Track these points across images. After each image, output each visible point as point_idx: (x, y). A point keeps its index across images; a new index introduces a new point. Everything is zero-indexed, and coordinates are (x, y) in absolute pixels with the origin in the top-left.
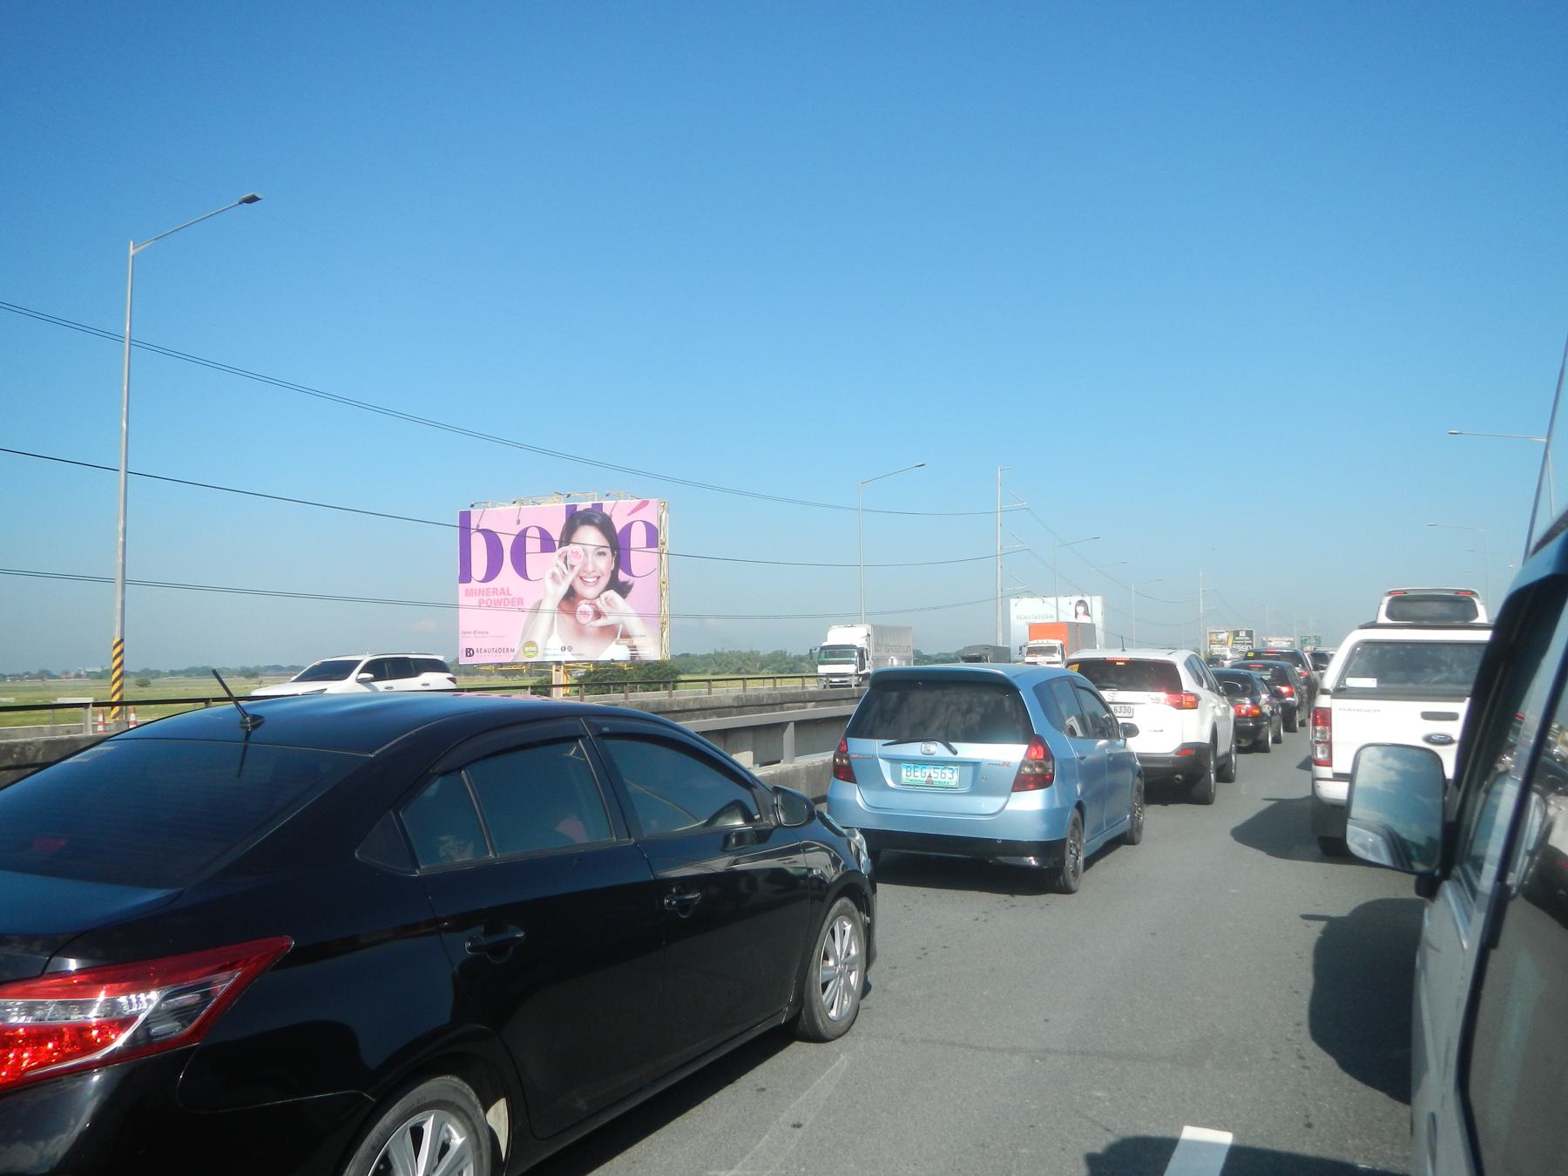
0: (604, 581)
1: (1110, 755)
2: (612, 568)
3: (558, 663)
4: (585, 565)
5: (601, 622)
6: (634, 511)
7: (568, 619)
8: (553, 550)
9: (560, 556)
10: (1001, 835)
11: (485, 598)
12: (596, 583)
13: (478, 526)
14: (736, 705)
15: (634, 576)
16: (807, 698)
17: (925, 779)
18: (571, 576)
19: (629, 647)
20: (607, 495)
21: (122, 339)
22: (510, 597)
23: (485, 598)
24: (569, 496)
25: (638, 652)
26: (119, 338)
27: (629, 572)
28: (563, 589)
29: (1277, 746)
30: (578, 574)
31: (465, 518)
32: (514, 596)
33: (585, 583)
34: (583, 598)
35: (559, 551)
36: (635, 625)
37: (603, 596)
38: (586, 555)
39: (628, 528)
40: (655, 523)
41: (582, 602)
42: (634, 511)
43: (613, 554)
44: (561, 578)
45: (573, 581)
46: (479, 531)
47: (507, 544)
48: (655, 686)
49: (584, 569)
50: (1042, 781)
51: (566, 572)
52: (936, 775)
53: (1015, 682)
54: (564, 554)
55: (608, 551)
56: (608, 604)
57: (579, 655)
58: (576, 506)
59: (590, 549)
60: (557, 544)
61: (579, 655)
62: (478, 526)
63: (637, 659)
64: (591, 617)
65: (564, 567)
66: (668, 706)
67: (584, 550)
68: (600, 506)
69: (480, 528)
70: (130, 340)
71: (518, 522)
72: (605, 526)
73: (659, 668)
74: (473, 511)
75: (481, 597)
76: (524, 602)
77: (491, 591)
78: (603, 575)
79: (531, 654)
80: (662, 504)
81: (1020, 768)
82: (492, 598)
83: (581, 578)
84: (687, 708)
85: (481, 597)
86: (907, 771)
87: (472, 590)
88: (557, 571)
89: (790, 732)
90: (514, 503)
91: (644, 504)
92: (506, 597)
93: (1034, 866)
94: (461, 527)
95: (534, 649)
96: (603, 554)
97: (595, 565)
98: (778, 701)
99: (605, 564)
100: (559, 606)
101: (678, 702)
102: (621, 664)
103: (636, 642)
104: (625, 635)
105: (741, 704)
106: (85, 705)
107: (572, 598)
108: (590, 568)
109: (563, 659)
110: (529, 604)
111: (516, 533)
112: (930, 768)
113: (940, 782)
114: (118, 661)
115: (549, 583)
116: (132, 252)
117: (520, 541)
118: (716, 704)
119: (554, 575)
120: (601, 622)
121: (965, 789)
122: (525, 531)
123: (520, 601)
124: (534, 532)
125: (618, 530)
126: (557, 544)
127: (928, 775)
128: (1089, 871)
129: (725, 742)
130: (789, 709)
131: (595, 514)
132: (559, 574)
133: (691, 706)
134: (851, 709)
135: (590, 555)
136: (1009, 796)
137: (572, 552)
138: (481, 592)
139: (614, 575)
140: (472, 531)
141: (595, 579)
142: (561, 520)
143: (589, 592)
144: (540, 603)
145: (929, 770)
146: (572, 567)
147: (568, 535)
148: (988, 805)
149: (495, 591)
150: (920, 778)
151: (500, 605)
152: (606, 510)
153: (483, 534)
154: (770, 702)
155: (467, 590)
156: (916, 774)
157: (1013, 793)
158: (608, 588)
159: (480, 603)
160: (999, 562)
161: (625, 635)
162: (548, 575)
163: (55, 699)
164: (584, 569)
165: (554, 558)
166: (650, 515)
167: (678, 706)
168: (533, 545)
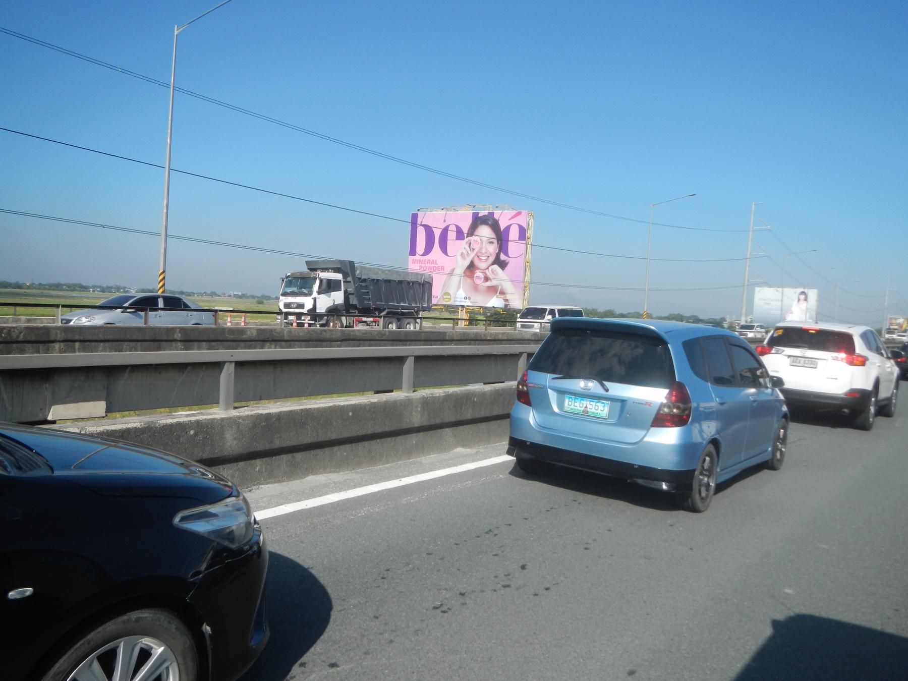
0: (492, 259)
1: (754, 401)
2: (497, 251)
3: (463, 306)
4: (481, 249)
5: (489, 284)
6: (513, 218)
7: (469, 280)
8: (463, 239)
9: (467, 242)
10: (639, 461)
11: (423, 265)
12: (486, 260)
13: (422, 222)
14: (533, 339)
15: (508, 256)
17: (582, 409)
18: (472, 255)
19: (504, 300)
20: (497, 207)
21: (169, 86)
22: (437, 266)
23: (423, 265)
24: (474, 206)
25: (510, 303)
26: (168, 86)
27: (507, 254)
29: (880, 419)
30: (476, 254)
31: (415, 217)
32: (438, 265)
33: (480, 260)
34: (478, 269)
35: (466, 240)
36: (508, 286)
38: (482, 243)
39: (508, 228)
40: (525, 226)
41: (477, 271)
42: (513, 218)
43: (498, 243)
44: (466, 256)
45: (473, 258)
46: (421, 225)
47: (437, 234)
50: (680, 420)
51: (469, 252)
52: (590, 407)
53: (666, 337)
55: (495, 241)
56: (493, 273)
57: (474, 302)
58: (478, 213)
59: (485, 239)
60: (465, 235)
61: (474, 302)
62: (422, 222)
63: (508, 307)
64: (482, 280)
65: (469, 250)
66: (483, 336)
67: (481, 240)
68: (492, 214)
69: (423, 224)
70: (174, 87)
71: (445, 221)
72: (495, 226)
74: (419, 213)
75: (421, 264)
76: (445, 269)
78: (491, 254)
79: (447, 300)
80: (530, 214)
81: (660, 409)
82: (427, 265)
83: (478, 257)
84: (496, 338)
85: (421, 264)
86: (569, 401)
87: (416, 260)
88: (464, 252)
90: (442, 209)
91: (519, 214)
92: (435, 265)
93: (664, 490)
94: (412, 223)
95: (449, 297)
96: (492, 243)
97: (486, 249)
99: (493, 249)
100: (464, 273)
101: (491, 334)
102: (499, 310)
103: (508, 297)
104: (502, 293)
105: (537, 339)
106: (57, 306)
107: (472, 268)
108: (484, 251)
109: (465, 304)
110: (447, 270)
112: (587, 401)
113: (593, 413)
114: (161, 284)
115: (459, 258)
116: (176, 32)
117: (445, 231)
118: (519, 337)
119: (462, 254)
120: (489, 284)
121: (612, 421)
123: (443, 268)
124: (452, 228)
125: (502, 228)
126: (465, 235)
127: (585, 406)
128: (720, 495)
131: (490, 219)
133: (500, 337)
134: (535, 348)
135: (484, 244)
136: (648, 430)
137: (474, 241)
138: (421, 262)
139: (498, 256)
140: (418, 225)
142: (469, 221)
143: (483, 265)
144: (453, 270)
145: (586, 402)
146: (473, 249)
147: (472, 232)
148: (631, 435)
149: (429, 262)
150: (578, 408)
151: (431, 270)
152: (496, 216)
153: (425, 229)
155: (413, 260)
156: (576, 404)
157: (652, 429)
158: (493, 263)
161: (502, 293)
163: (214, 307)
165: (463, 244)
166: (522, 220)
167: (491, 337)
168: (452, 235)
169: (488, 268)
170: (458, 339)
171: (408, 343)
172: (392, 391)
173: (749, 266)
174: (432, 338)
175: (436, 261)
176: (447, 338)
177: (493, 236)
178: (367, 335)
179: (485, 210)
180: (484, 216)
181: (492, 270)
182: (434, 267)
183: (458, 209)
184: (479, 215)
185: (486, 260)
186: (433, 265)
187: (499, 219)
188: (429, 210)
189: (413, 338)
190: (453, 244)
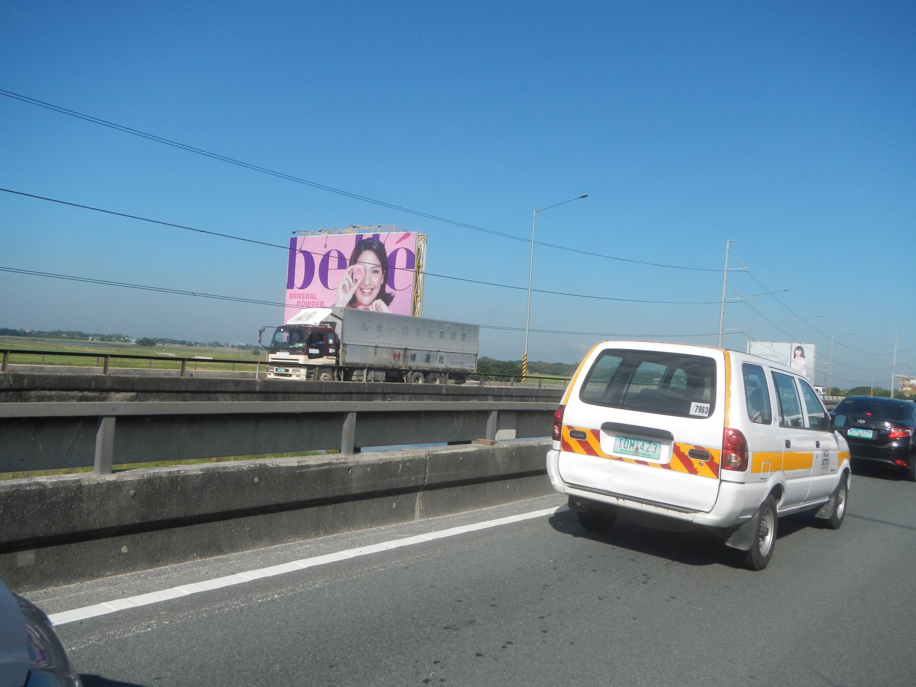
0: (376, 292)
2: (382, 283)
4: (364, 279)
9: (349, 272)
12: (370, 293)
13: (301, 248)
15: (395, 289)
16: (108, 385)
18: (355, 287)
22: (316, 301)
27: (392, 287)
28: (349, 297)
30: (359, 287)
31: (294, 241)
33: (363, 293)
34: (361, 304)
35: (349, 269)
37: (374, 303)
38: (366, 272)
39: (395, 253)
40: (413, 250)
43: (383, 272)
44: (348, 288)
45: (356, 291)
46: (301, 251)
47: (317, 261)
48: (507, 378)
49: (363, 283)
51: (352, 284)
54: (352, 272)
55: (380, 269)
58: (362, 236)
59: (369, 267)
60: (348, 262)
62: (301, 248)
68: (377, 237)
69: (302, 250)
71: (326, 246)
73: (511, 368)
75: (299, 300)
77: (305, 295)
78: (375, 287)
82: (305, 300)
83: (361, 289)
85: (299, 300)
88: (346, 283)
89: (349, 424)
90: (320, 231)
91: (407, 235)
92: (314, 300)
96: (376, 272)
97: (370, 280)
99: (377, 280)
107: (354, 304)
108: (367, 282)
111: (324, 254)
115: (340, 291)
117: (326, 257)
119: (344, 286)
122: (329, 253)
124: (334, 254)
125: (388, 254)
126: (348, 262)
130: (40, 399)
132: (347, 286)
135: (368, 273)
138: (299, 296)
139: (383, 288)
140: (297, 252)
141: (370, 291)
142: (352, 246)
146: (356, 280)
147: (355, 259)
152: (382, 240)
158: (378, 297)
159: (298, 303)
160: (723, 309)
162: (340, 286)
164: (363, 283)
165: (345, 273)
166: (411, 244)
168: (333, 263)
169: (371, 303)
173: (724, 313)
175: (315, 295)
177: (378, 263)
179: (369, 231)
180: (369, 239)
181: (376, 306)
182: (313, 302)
183: (341, 232)
184: (363, 239)
185: (370, 293)
186: (311, 300)
187: (384, 243)
188: (309, 233)
190: (334, 274)
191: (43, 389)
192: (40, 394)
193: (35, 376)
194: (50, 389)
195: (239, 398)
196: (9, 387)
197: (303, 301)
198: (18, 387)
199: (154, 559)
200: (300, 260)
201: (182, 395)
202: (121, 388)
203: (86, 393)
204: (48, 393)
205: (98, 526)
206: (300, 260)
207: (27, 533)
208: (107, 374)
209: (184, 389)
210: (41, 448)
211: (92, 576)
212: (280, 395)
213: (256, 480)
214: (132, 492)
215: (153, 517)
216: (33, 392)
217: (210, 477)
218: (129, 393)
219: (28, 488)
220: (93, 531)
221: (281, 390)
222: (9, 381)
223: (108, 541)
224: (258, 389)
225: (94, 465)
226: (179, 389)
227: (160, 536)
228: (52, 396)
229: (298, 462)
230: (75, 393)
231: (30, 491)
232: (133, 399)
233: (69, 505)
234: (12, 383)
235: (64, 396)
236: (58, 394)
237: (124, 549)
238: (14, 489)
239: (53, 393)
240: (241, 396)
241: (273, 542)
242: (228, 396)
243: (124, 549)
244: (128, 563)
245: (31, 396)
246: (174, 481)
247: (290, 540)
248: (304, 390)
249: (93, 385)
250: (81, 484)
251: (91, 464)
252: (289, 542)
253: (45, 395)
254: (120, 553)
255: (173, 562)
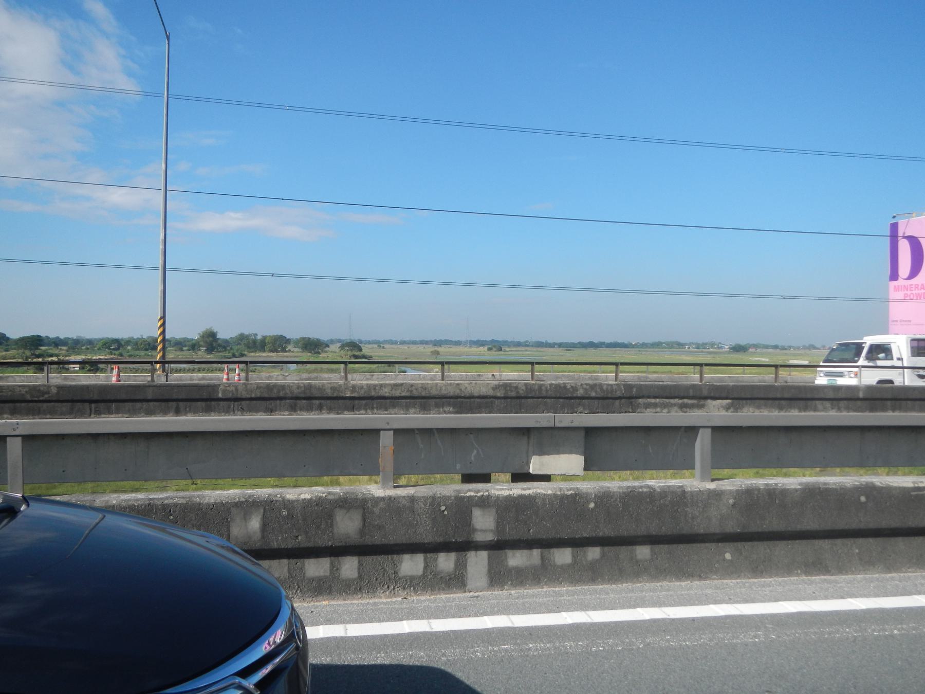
11: (909, 292)
13: (904, 233)
21: (162, 95)
23: (909, 292)
31: (894, 227)
46: (904, 237)
62: (904, 233)
69: (906, 235)
77: (913, 286)
82: (914, 292)
84: (373, 394)
87: (898, 286)
94: (891, 236)
98: (618, 394)
118: (451, 391)
129: (529, 438)
133: (386, 392)
138: (906, 288)
140: (899, 238)
149: (917, 286)
153: (907, 240)
154: (593, 394)
155: (895, 286)
159: (905, 297)
167: (352, 392)
170: (253, 396)
171: (114, 405)
172: (485, 478)
174: (175, 396)
176: (220, 395)
178: (4, 394)
188: (914, 215)
189: (123, 396)
191: (649, 397)
192: (646, 401)
193: (642, 385)
194: (655, 397)
195: (840, 405)
196: (622, 396)
197: (912, 294)
198: (628, 396)
199: (758, 569)
200: (904, 248)
201: (777, 402)
202: (717, 395)
203: (686, 401)
204: (653, 401)
205: (702, 531)
206: (904, 248)
207: (642, 530)
208: (703, 382)
209: (779, 396)
210: (651, 451)
211: (700, 578)
212: (889, 403)
213: (863, 499)
214: (731, 501)
215: (753, 529)
216: (640, 400)
217: (811, 493)
218: (725, 401)
219: (640, 490)
220: (698, 535)
221: (889, 397)
222: (621, 391)
223: (712, 546)
224: (861, 395)
225: (694, 469)
226: (774, 397)
227: (762, 548)
228: (657, 404)
229: (914, 483)
230: (676, 401)
231: (642, 492)
232: (727, 408)
233: (676, 508)
234: (623, 391)
235: (667, 403)
236: (661, 402)
237: (728, 556)
238: (629, 490)
239: (658, 400)
240: (842, 404)
241: (889, 569)
242: (828, 404)
243: (728, 556)
244: (732, 570)
245: (639, 404)
246: (772, 494)
247: (910, 570)
248: (918, 397)
249: (691, 393)
250: (684, 490)
251: (692, 467)
252: (910, 572)
253: (651, 403)
254: (724, 560)
255: (777, 575)
